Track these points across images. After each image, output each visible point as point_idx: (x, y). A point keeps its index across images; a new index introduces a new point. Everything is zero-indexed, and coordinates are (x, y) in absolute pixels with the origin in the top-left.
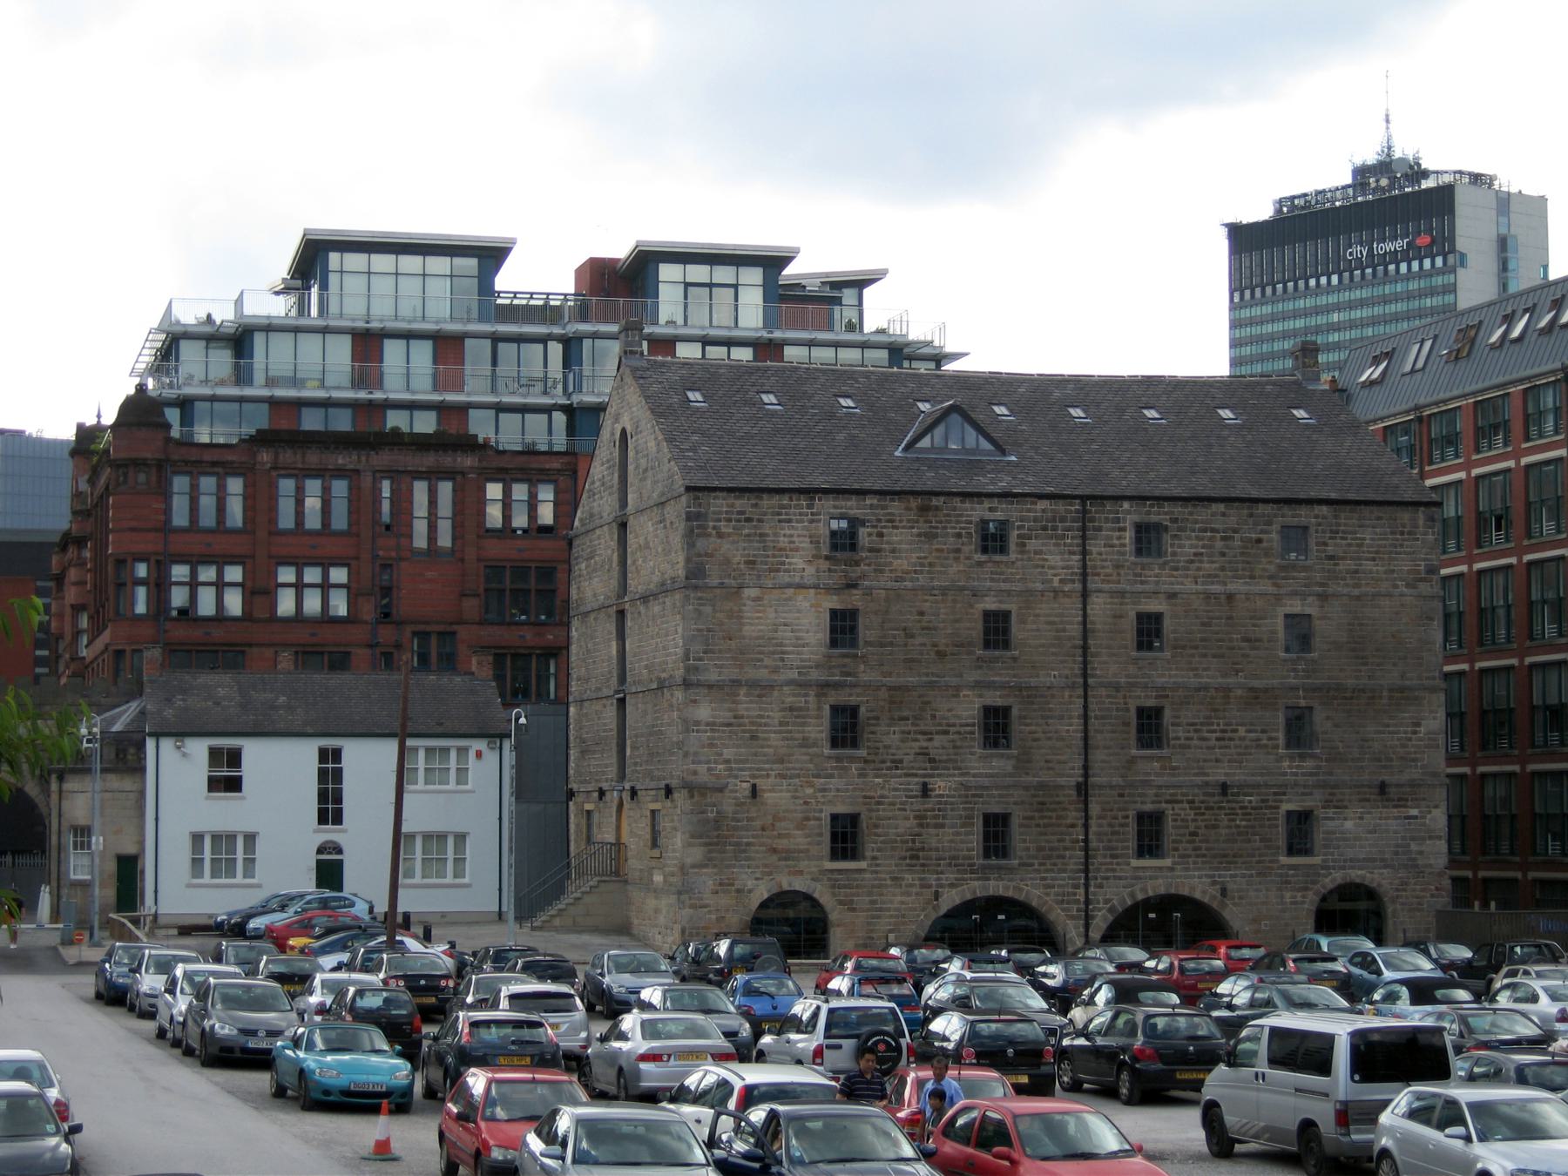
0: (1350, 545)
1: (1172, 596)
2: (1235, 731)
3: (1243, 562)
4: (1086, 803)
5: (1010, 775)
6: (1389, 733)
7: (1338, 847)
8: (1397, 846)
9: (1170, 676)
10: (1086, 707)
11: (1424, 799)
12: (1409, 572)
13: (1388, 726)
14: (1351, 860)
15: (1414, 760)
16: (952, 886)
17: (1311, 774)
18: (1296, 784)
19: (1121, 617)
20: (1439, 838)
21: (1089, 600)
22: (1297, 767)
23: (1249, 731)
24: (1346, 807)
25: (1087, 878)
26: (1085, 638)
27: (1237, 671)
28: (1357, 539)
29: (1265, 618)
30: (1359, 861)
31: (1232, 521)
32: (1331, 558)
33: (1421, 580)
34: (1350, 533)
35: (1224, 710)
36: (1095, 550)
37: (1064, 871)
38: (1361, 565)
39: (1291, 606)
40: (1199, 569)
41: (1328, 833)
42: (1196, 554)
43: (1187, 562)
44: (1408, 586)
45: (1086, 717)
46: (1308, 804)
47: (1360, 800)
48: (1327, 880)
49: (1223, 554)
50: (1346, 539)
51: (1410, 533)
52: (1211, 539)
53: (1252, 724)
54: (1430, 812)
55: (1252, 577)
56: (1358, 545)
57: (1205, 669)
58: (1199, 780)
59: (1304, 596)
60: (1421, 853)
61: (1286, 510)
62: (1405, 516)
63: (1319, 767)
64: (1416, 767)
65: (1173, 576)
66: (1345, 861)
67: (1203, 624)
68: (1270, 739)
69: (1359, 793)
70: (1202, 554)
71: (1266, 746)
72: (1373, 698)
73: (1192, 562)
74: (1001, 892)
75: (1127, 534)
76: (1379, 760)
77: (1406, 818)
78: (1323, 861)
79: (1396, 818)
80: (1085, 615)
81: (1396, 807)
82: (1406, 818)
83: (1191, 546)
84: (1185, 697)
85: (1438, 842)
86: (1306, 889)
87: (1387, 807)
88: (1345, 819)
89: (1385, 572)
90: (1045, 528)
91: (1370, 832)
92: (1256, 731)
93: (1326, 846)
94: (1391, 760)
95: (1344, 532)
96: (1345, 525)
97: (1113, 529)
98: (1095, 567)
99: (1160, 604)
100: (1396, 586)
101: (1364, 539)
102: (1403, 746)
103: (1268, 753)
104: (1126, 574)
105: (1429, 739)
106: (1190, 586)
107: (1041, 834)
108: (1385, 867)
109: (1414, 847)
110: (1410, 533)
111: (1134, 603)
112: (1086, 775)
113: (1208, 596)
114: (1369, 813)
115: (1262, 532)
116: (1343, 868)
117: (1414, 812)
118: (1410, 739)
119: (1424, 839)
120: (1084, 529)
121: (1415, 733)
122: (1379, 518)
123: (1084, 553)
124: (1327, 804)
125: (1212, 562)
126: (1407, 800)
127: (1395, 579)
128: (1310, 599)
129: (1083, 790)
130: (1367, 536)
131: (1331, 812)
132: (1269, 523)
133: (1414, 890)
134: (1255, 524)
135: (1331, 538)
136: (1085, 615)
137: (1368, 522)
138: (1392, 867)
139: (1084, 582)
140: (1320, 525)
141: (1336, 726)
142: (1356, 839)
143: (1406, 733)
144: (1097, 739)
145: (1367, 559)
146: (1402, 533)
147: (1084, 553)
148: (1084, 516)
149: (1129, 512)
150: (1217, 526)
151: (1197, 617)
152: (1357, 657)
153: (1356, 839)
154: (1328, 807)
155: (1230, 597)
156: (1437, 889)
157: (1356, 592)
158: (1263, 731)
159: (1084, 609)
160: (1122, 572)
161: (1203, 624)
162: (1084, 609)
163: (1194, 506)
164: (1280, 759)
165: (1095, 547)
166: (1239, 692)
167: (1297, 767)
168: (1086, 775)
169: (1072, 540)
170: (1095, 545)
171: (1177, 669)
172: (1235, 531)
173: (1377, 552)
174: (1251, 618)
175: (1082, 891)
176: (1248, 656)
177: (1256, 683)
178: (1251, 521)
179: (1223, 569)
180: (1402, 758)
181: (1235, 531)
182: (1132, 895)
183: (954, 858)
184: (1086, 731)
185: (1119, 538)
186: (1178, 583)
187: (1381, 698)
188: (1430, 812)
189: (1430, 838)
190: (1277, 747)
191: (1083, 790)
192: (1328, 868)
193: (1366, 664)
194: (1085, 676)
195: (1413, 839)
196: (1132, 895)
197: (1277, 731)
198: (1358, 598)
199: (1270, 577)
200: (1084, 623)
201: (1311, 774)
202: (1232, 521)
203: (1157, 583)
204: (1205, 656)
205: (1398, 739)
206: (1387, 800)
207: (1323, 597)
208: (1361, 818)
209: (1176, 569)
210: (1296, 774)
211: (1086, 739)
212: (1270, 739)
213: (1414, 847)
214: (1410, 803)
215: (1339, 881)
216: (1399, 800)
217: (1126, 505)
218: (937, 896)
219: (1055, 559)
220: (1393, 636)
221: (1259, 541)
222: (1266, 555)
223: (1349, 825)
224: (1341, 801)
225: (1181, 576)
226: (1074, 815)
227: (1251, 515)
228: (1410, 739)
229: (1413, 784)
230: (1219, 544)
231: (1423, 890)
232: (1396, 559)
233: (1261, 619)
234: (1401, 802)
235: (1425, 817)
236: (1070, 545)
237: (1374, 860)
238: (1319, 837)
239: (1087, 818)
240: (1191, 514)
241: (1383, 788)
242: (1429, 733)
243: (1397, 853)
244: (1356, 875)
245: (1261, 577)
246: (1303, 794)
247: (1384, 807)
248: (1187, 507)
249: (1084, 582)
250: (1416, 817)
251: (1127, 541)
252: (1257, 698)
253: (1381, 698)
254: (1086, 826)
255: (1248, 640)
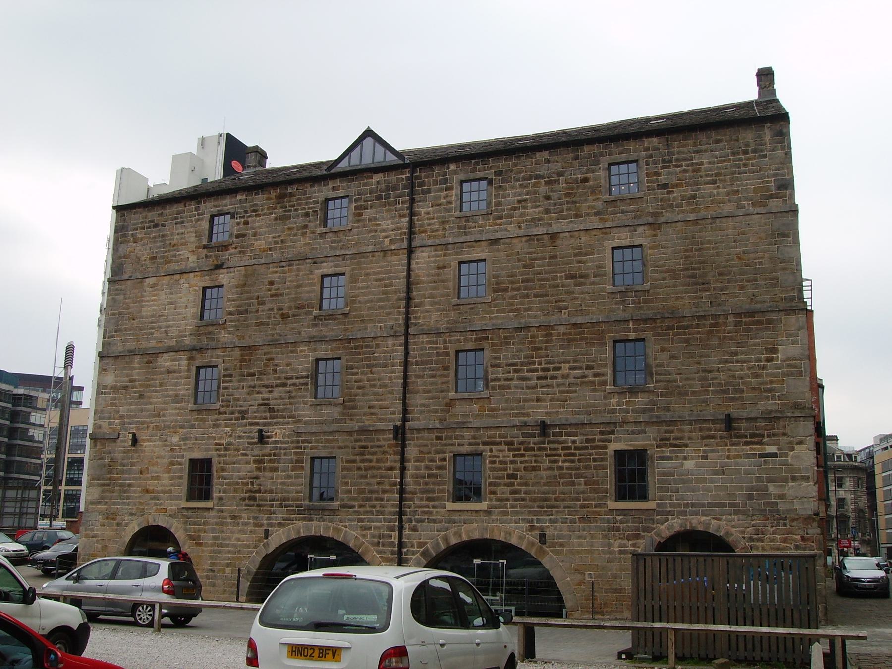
0: (685, 171)
1: (495, 242)
2: (559, 368)
3: (568, 202)
4: (404, 446)
5: (338, 421)
6: (738, 362)
7: (678, 491)
8: (752, 488)
9: (491, 318)
10: (407, 353)
11: (784, 434)
12: (755, 190)
13: (736, 354)
14: (693, 505)
15: (770, 390)
16: (280, 525)
17: (644, 411)
18: (624, 423)
19: (444, 267)
20: (807, 479)
21: (413, 256)
22: (628, 403)
23: (572, 368)
24: (686, 446)
25: (401, 521)
26: (409, 290)
27: (560, 309)
28: (692, 164)
29: (593, 254)
30: (703, 505)
31: (557, 166)
32: (665, 186)
33: (771, 197)
34: (685, 159)
35: (546, 349)
36: (423, 211)
37: (382, 513)
38: (699, 189)
39: (619, 238)
40: (522, 215)
41: (664, 474)
42: (519, 202)
43: (512, 209)
44: (754, 205)
45: (406, 364)
46: (639, 442)
47: (703, 438)
48: (662, 527)
49: (548, 198)
50: (681, 166)
51: (755, 151)
52: (535, 185)
53: (575, 361)
54: (793, 449)
55: (577, 216)
56: (694, 171)
57: (526, 310)
58: (517, 421)
59: (633, 227)
60: (782, 497)
61: (613, 147)
62: (748, 136)
63: (654, 403)
64: (773, 398)
65: (496, 224)
66: (686, 506)
67: (525, 266)
68: (596, 375)
69: (701, 430)
70: (526, 200)
71: (593, 383)
72: (716, 325)
73: (515, 209)
74: (322, 533)
75: (454, 192)
76: (725, 392)
77: (761, 456)
78: (658, 505)
79: (748, 456)
80: (409, 269)
81: (747, 443)
82: (761, 456)
83: (515, 195)
84: (506, 338)
85: (805, 484)
86: (637, 537)
87: (737, 444)
88: (685, 458)
89: (728, 194)
90: (379, 198)
91: (716, 473)
92: (581, 368)
93: (661, 489)
94: (742, 391)
95: (677, 160)
96: (679, 153)
97: (441, 190)
98: (422, 226)
99: (483, 251)
100: (740, 207)
101: (702, 163)
102: (757, 376)
103: (594, 390)
104: (452, 228)
105: (789, 366)
106: (513, 230)
107: (362, 477)
108: (736, 513)
109: (772, 489)
110: (755, 151)
111: (457, 254)
112: (405, 420)
113: (530, 238)
114: (713, 451)
115: (588, 171)
116: (684, 513)
117: (772, 449)
118: (764, 368)
119: (786, 480)
120: (412, 194)
121: (769, 360)
122: (718, 141)
123: (412, 214)
124: (663, 442)
125: (537, 207)
126: (763, 436)
127: (740, 199)
128: (640, 230)
129: (400, 433)
130: (705, 159)
131: (667, 452)
132: (596, 163)
133: (772, 540)
134: (581, 166)
135: (663, 168)
136: (409, 269)
137: (704, 147)
138: (745, 513)
139: (410, 240)
140: (651, 156)
141: (673, 357)
142: (698, 481)
143: (759, 360)
144: (418, 384)
145: (706, 183)
146: (746, 152)
147: (412, 214)
148: (412, 185)
149: (455, 172)
150: (541, 173)
151: (519, 260)
152: (697, 284)
153: (698, 481)
154: (665, 446)
155: (553, 236)
156: (803, 539)
157: (692, 217)
158: (589, 368)
159: (409, 264)
160: (447, 227)
161: (525, 266)
162: (409, 264)
163: (518, 157)
164: (608, 396)
165: (423, 209)
166: (562, 329)
167: (628, 403)
168: (405, 420)
169: (403, 206)
170: (423, 207)
171: (497, 311)
172: (560, 174)
173: (716, 175)
174: (576, 255)
175: (395, 534)
176: (573, 293)
177: (580, 320)
178: (576, 163)
179: (547, 211)
180: (754, 389)
181: (560, 174)
182: (446, 539)
183: (284, 499)
184: (406, 377)
185: (446, 197)
186: (501, 230)
187: (726, 324)
188: (793, 449)
189: (794, 479)
190: (604, 383)
191: (400, 433)
192: (665, 513)
193: (707, 290)
194: (407, 326)
195: (770, 480)
196: (446, 539)
197: (605, 366)
198: (695, 222)
199: (596, 214)
200: (409, 276)
201: (644, 411)
202: (557, 166)
203: (481, 232)
204: (527, 296)
205: (749, 369)
206: (737, 436)
207: (655, 226)
208: (705, 457)
209: (500, 218)
210: (627, 411)
211: (405, 384)
212: (596, 375)
213: (772, 489)
214: (766, 439)
215: (677, 528)
216: (753, 435)
217: (453, 167)
218: (267, 534)
219: (387, 224)
220: (739, 258)
221: (586, 180)
222: (593, 193)
223: (689, 464)
224: (681, 438)
225: (505, 224)
226: (393, 459)
227: (576, 158)
228: (764, 368)
229: (770, 418)
230: (543, 189)
231: (785, 540)
232: (738, 179)
233: (586, 255)
234: (755, 438)
235: (787, 455)
236: (401, 209)
237: (722, 505)
238: (653, 481)
239: (403, 460)
240: (516, 165)
241: (729, 422)
242: (789, 359)
243: (750, 497)
244: (698, 522)
245: (588, 214)
246: (633, 432)
247: (732, 445)
248: (511, 159)
249: (410, 240)
250: (774, 455)
251: (454, 198)
252: (582, 333)
253: (726, 324)
254: (403, 469)
255: (573, 277)
